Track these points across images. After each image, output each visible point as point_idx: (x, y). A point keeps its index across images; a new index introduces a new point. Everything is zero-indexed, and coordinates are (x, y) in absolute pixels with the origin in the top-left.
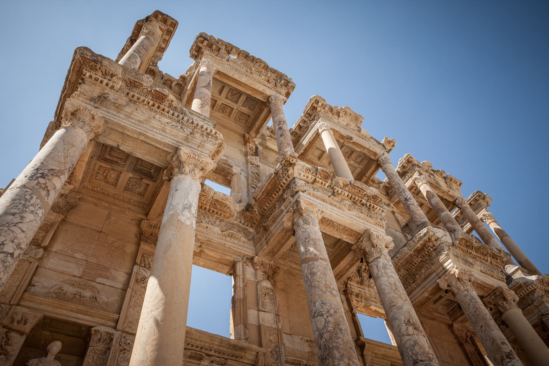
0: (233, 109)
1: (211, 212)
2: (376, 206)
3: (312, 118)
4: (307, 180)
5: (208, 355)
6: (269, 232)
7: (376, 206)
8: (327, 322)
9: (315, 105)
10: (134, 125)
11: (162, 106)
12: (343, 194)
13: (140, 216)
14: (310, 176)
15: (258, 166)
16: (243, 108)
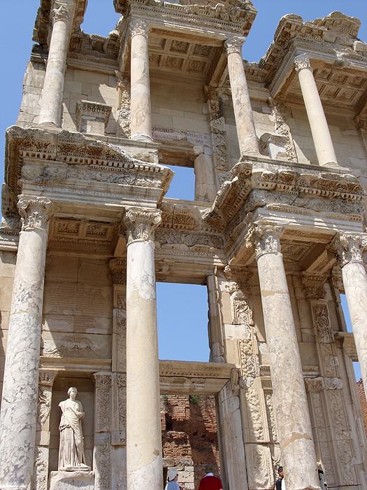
0: (183, 59)
1: (174, 227)
2: (352, 195)
3: (286, 47)
4: (267, 188)
5: (188, 378)
6: (236, 243)
7: (352, 195)
8: (279, 359)
9: (286, 30)
10: (80, 197)
11: (100, 161)
12: (311, 192)
13: (106, 256)
14: (270, 184)
15: (223, 133)
16: (194, 56)
